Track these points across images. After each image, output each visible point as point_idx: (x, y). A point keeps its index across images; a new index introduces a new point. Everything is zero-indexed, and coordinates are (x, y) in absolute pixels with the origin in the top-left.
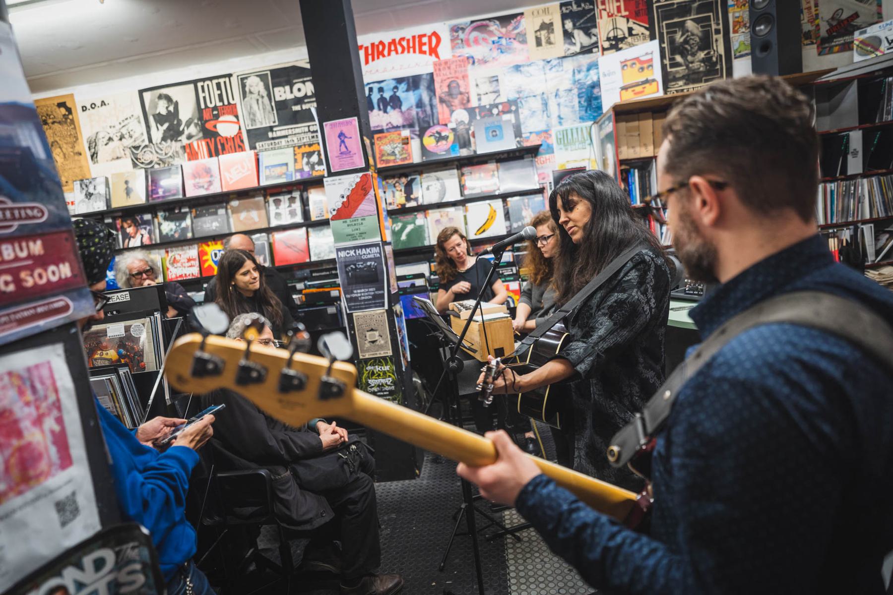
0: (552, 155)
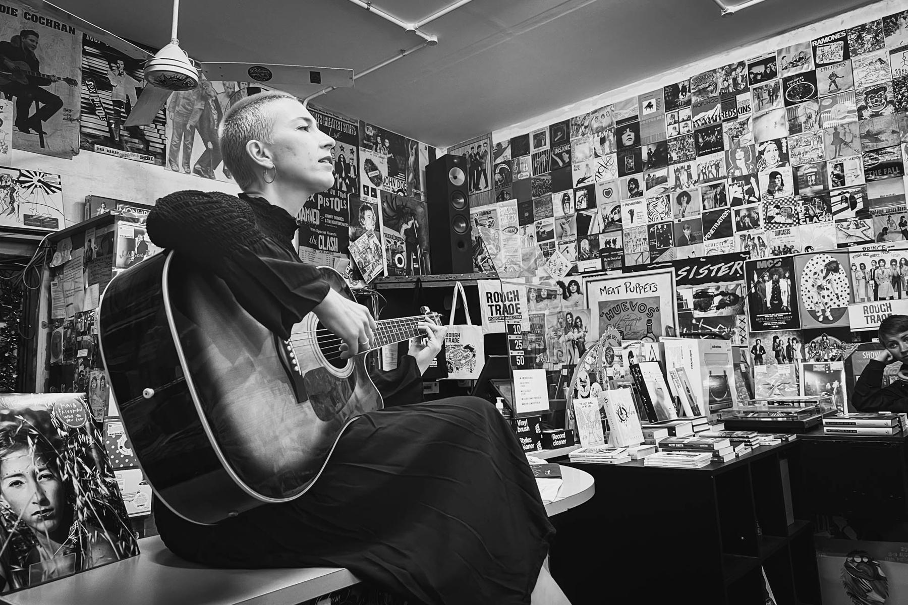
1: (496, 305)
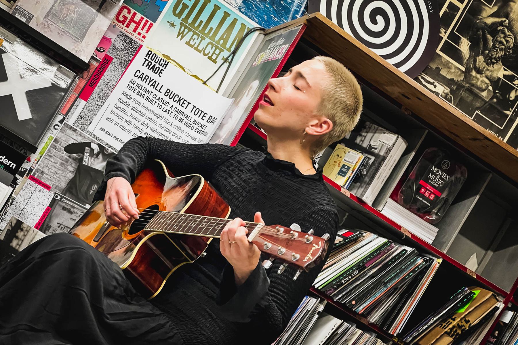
0: (150, 22)
1: (150, 62)
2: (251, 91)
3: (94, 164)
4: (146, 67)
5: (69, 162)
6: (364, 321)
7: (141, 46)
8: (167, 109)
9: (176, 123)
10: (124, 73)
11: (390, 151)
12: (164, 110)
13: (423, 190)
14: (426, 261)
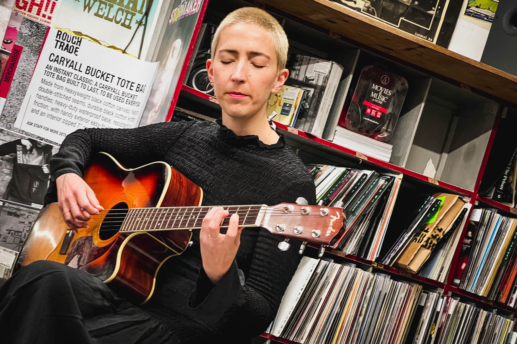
1: (62, 42)
2: (175, 51)
3: (29, 161)
4: (59, 48)
5: (3, 164)
6: (340, 254)
7: (49, 28)
8: (92, 87)
9: (105, 99)
10: (38, 60)
11: (328, 79)
12: (89, 89)
13: (369, 111)
14: (388, 180)
